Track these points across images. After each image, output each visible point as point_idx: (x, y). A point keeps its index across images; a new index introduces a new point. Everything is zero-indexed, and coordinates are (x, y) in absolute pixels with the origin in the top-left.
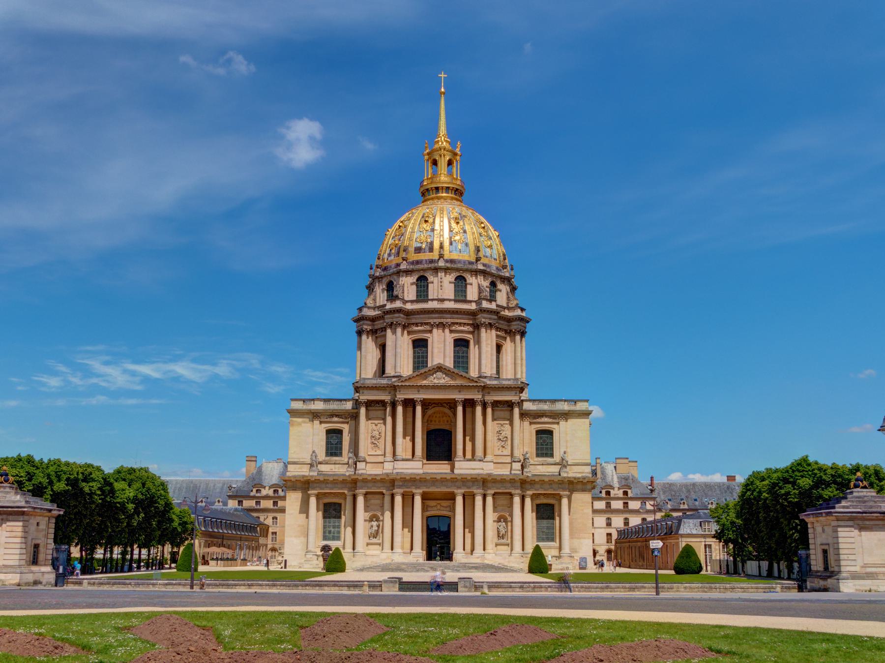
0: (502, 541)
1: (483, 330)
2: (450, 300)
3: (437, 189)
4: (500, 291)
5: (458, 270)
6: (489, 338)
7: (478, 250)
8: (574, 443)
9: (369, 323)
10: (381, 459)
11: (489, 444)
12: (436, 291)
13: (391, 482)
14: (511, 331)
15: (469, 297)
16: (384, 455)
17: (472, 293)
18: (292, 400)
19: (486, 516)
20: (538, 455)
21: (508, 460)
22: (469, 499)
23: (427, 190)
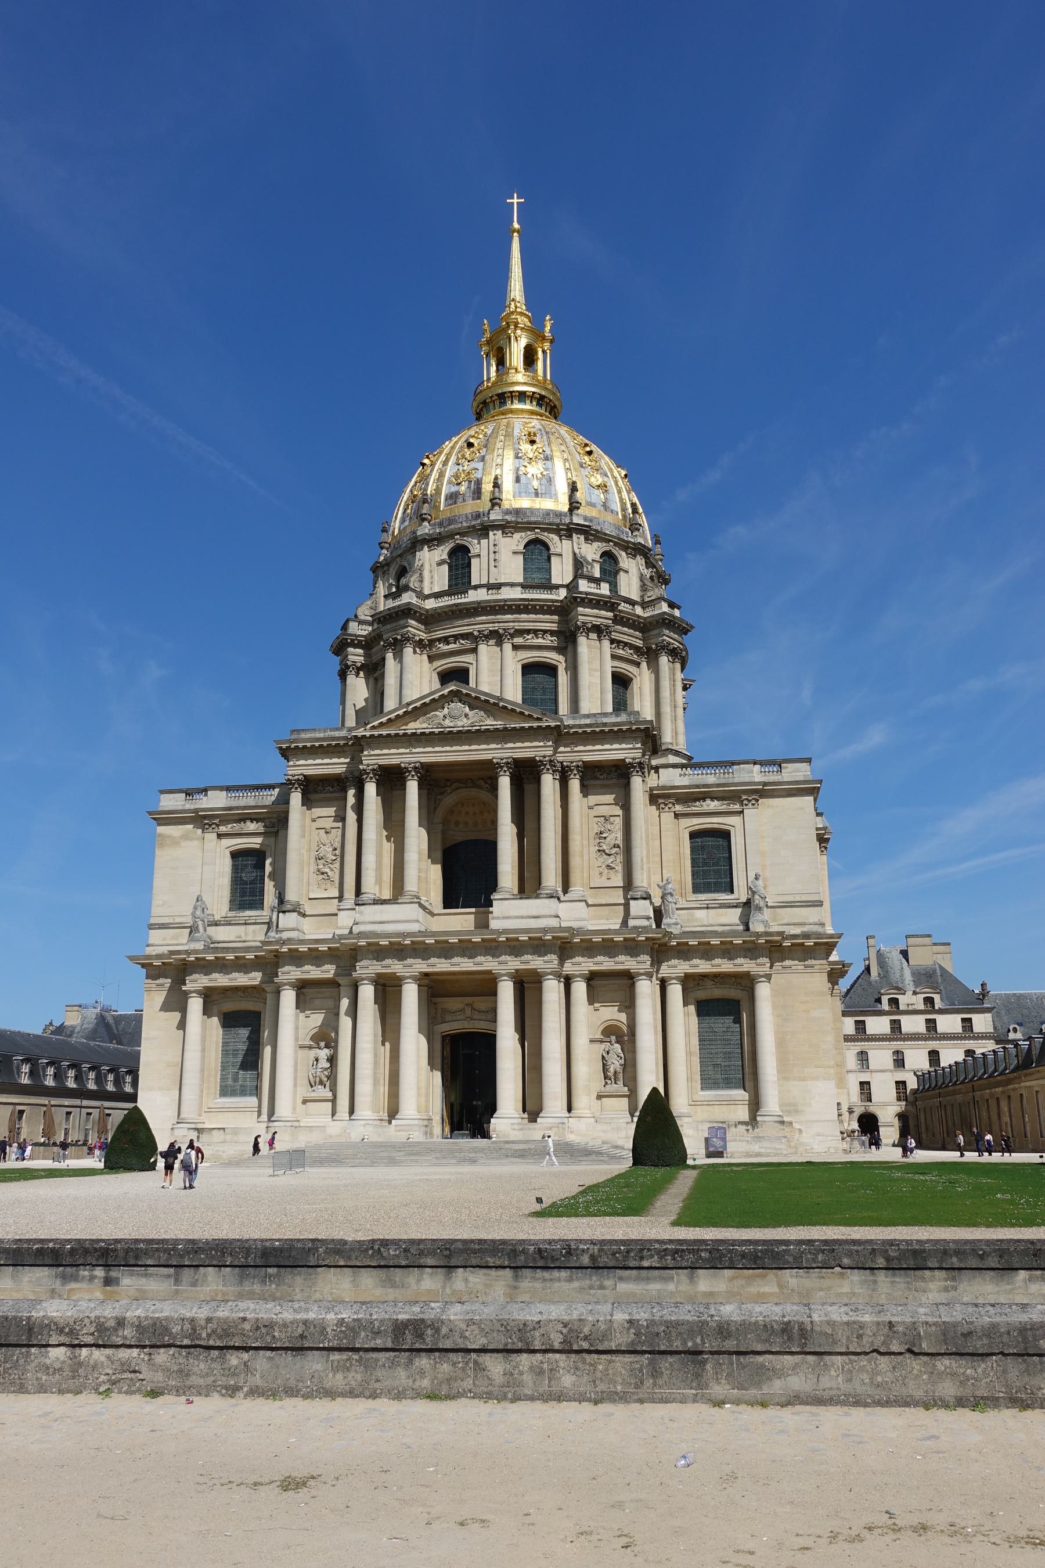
0: (612, 1088)
1: (582, 640)
2: (512, 585)
3: (502, 398)
4: (626, 572)
5: (529, 527)
6: (595, 660)
7: (573, 488)
8: (780, 851)
9: (360, 651)
10: (332, 906)
11: (575, 861)
12: (485, 573)
13: (346, 955)
14: (649, 649)
15: (555, 580)
16: (341, 898)
17: (561, 571)
18: (162, 792)
19: (571, 1023)
20: (697, 889)
21: (619, 897)
22: (528, 988)
23: (484, 403)
